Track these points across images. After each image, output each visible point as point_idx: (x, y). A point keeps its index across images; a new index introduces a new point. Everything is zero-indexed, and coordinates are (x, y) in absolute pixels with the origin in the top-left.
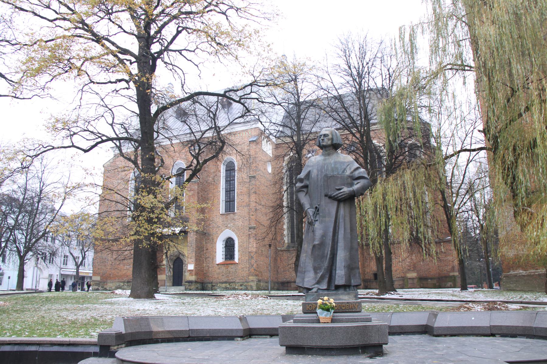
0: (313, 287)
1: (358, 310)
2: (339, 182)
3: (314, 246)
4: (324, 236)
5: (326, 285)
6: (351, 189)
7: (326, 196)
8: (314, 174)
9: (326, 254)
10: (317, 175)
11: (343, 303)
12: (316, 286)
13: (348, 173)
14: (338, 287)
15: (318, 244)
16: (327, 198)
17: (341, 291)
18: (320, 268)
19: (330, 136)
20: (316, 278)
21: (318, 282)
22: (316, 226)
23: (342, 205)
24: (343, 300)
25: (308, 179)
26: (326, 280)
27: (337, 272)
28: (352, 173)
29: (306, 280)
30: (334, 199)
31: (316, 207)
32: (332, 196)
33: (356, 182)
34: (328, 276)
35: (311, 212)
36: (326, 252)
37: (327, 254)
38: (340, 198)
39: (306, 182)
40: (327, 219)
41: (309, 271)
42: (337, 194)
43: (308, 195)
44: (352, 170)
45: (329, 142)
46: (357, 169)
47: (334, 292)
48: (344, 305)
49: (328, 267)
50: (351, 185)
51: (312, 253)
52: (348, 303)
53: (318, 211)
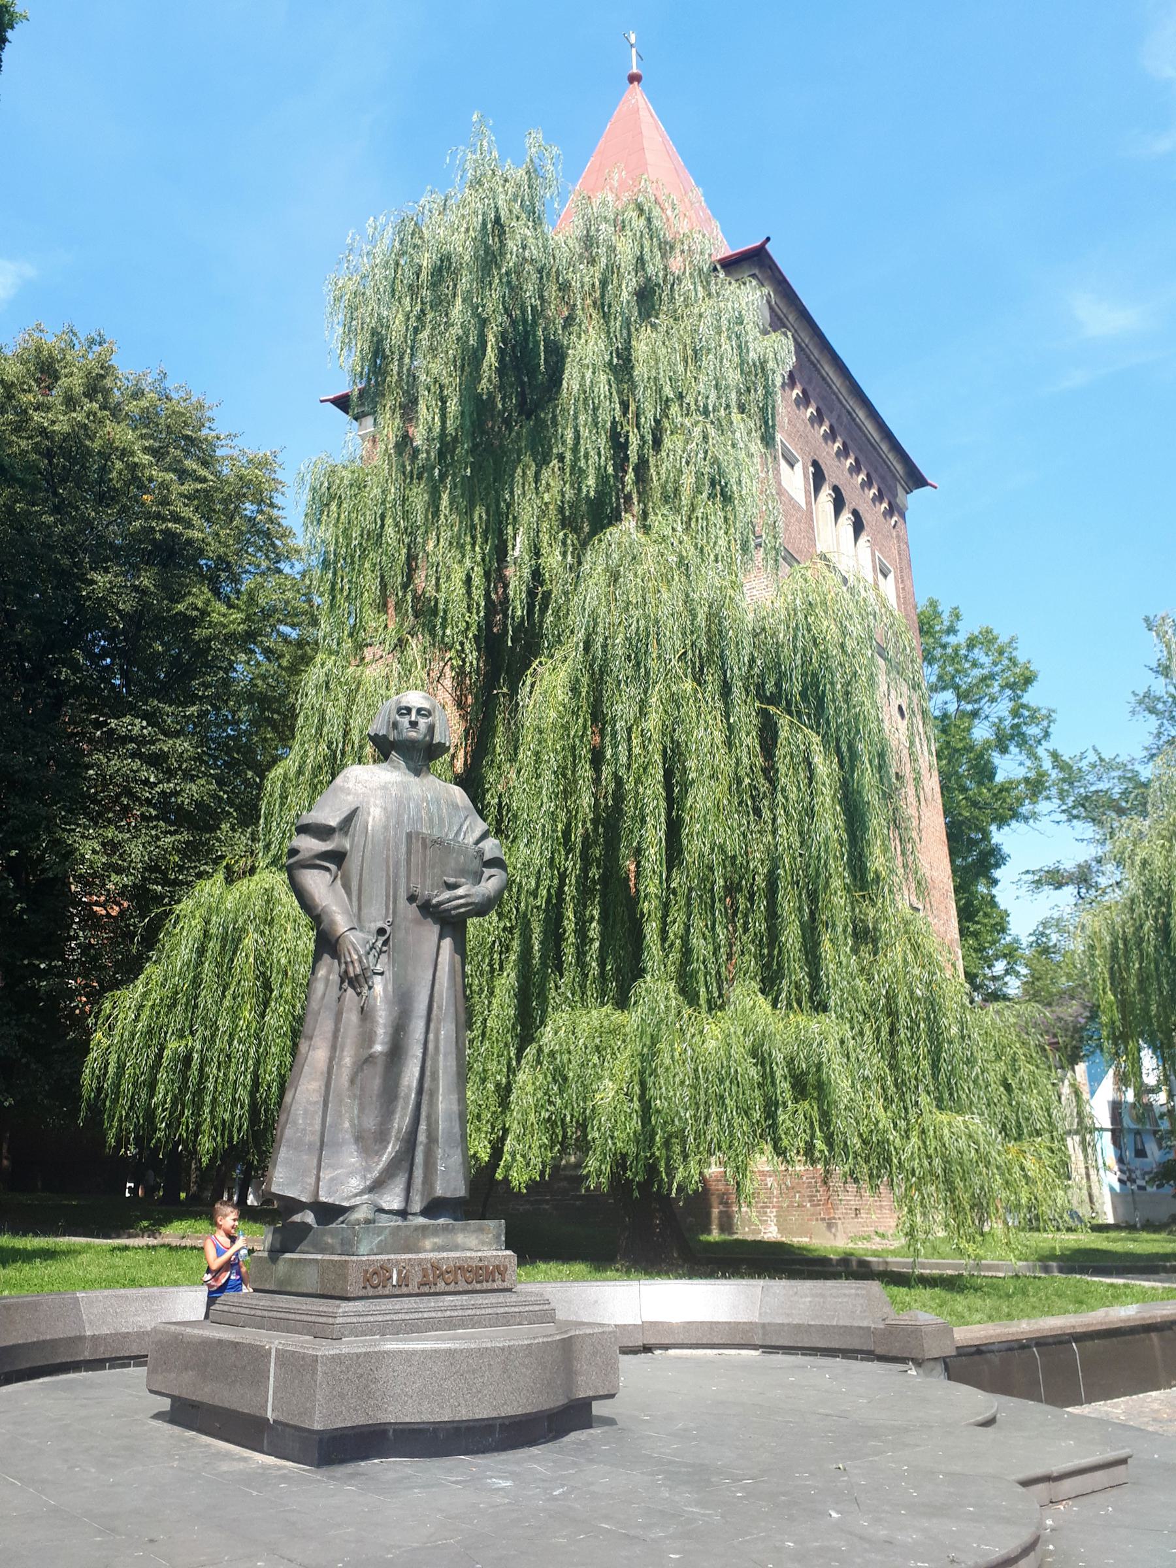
0: (353, 1202)
8: (374, 816)
10: (386, 828)
18: (382, 1137)
21: (376, 1186)
28: (477, 843)
31: (381, 931)
34: (406, 1165)
42: (449, 900)
50: (477, 878)
51: (352, 1082)
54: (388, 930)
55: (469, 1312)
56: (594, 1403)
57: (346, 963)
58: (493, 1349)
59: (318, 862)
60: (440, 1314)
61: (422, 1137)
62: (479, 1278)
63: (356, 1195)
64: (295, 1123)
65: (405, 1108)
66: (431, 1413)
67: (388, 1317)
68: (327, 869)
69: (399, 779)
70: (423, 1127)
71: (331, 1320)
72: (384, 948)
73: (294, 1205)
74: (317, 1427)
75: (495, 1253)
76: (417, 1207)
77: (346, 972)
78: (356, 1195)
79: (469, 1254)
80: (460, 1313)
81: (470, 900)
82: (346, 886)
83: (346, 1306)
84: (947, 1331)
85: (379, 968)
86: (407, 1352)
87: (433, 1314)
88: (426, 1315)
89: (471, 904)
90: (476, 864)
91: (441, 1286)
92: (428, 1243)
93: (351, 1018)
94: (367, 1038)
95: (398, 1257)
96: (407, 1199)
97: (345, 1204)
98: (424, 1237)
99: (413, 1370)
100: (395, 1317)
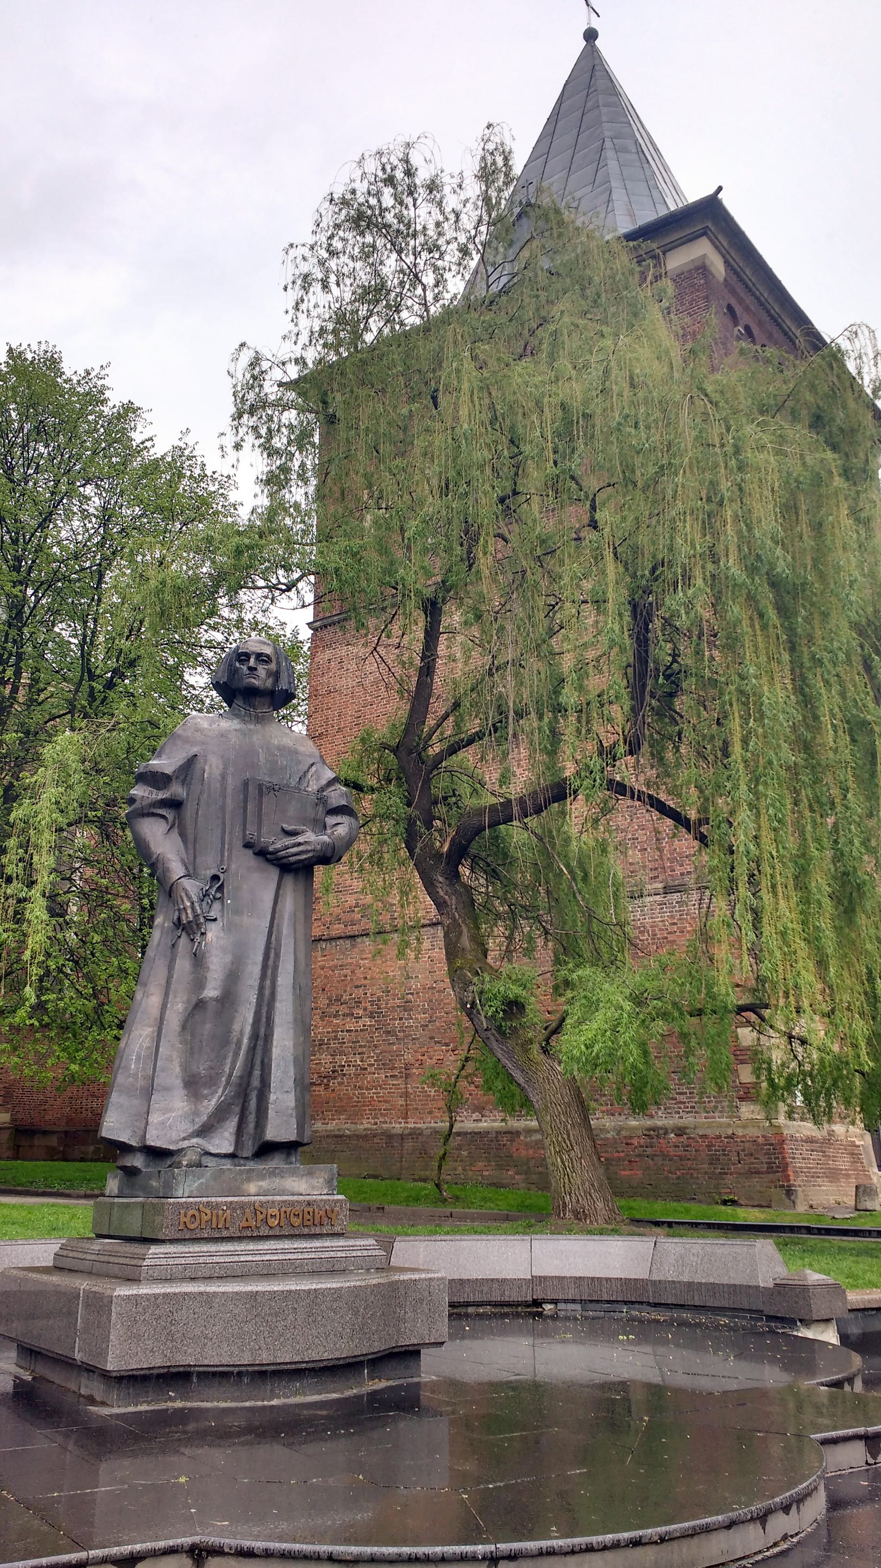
1: (338, 1229)
2: (292, 809)
3: (199, 1005)
4: (233, 977)
5: (232, 1139)
6: (325, 838)
7: (248, 845)
8: (212, 767)
9: (235, 1035)
10: (223, 777)
11: (292, 1204)
12: (194, 1141)
13: (313, 787)
14: (266, 1150)
15: (216, 1000)
16: (250, 852)
17: (276, 1162)
18: (212, 1081)
19: (273, 666)
20: (196, 1113)
21: (204, 1131)
22: (210, 936)
23: (289, 881)
25: (183, 783)
26: (231, 1125)
27: (272, 1097)
28: (322, 789)
29: (155, 1118)
30: (268, 861)
31: (215, 878)
32: (271, 849)
33: (331, 820)
34: (237, 1109)
35: (192, 887)
36: (236, 1027)
37: (242, 1033)
39: (177, 790)
40: (246, 920)
41: (167, 1089)
43: (176, 830)
44: (324, 782)
45: (269, 683)
47: (251, 1165)
48: (298, 1209)
49: (241, 1077)
51: (184, 1028)
52: (309, 1204)
53: (220, 889)
54: (222, 876)
56: (423, 1351)
57: (179, 910)
61: (256, 1082)
62: (306, 1223)
63: (184, 1139)
64: (127, 1068)
65: (236, 1054)
66: (231, 1356)
67: (201, 1260)
68: (163, 817)
69: (238, 727)
70: (257, 1073)
71: (139, 1263)
72: (219, 895)
73: (125, 1148)
74: (109, 1367)
76: (248, 1152)
77: (179, 919)
78: (184, 1139)
80: (281, 1257)
81: (309, 848)
82: (183, 835)
83: (154, 1249)
84: (837, 1290)
85: (213, 914)
86: (208, 1293)
87: (250, 1258)
88: (242, 1259)
89: (308, 851)
91: (264, 1231)
92: (252, 1188)
93: (183, 964)
94: (199, 984)
95: (219, 1199)
96: (238, 1142)
98: (249, 1180)
99: (212, 1312)
100: (209, 1260)
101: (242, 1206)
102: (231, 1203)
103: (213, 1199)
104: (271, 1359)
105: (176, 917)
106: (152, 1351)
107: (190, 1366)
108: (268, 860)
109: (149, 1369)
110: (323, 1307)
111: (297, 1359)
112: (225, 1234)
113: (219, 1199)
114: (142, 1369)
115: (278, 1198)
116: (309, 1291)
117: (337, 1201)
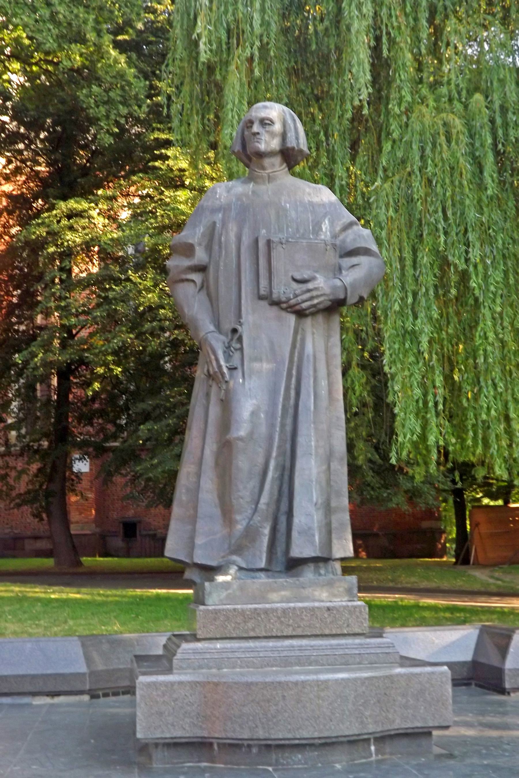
14: (294, 565)
20: (230, 535)
24: (314, 600)
30: (285, 309)
38: (304, 305)
46: (351, 225)
52: (328, 609)
55: (307, 653)
58: (287, 683)
59: (184, 277)
60: (276, 654)
75: (344, 604)
77: (208, 371)
79: (317, 604)
80: (298, 653)
88: (261, 655)
90: (332, 258)
95: (245, 606)
96: (270, 558)
97: (214, 563)
100: (230, 655)
101: (266, 611)
102: (255, 609)
103: (239, 607)
104: (267, 735)
105: (206, 370)
106: (173, 725)
107: (205, 738)
108: (282, 309)
109: (172, 738)
110: (312, 696)
111: (290, 736)
112: (252, 634)
113: (245, 606)
114: (166, 738)
115: (300, 605)
116: (296, 683)
117: (355, 607)
